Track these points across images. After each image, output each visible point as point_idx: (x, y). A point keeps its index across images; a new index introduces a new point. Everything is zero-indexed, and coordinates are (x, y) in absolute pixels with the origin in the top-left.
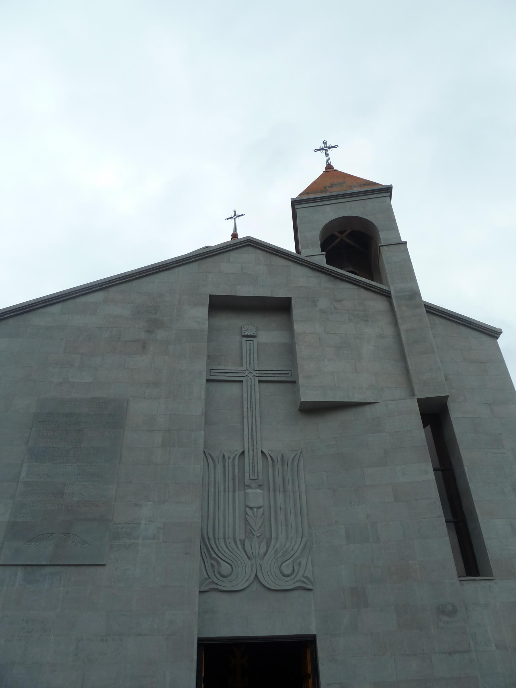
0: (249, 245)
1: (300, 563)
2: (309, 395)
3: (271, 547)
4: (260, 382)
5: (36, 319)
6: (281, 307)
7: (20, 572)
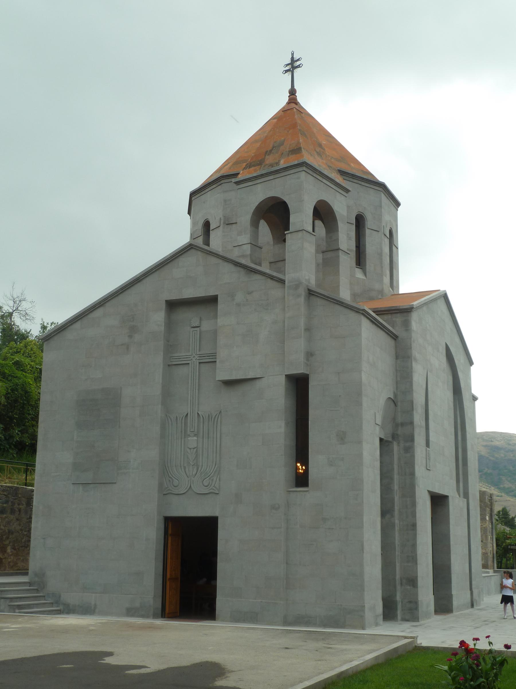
0: (192, 248)
1: (213, 480)
3: (199, 471)
4: (199, 363)
5: (69, 335)
7: (81, 487)
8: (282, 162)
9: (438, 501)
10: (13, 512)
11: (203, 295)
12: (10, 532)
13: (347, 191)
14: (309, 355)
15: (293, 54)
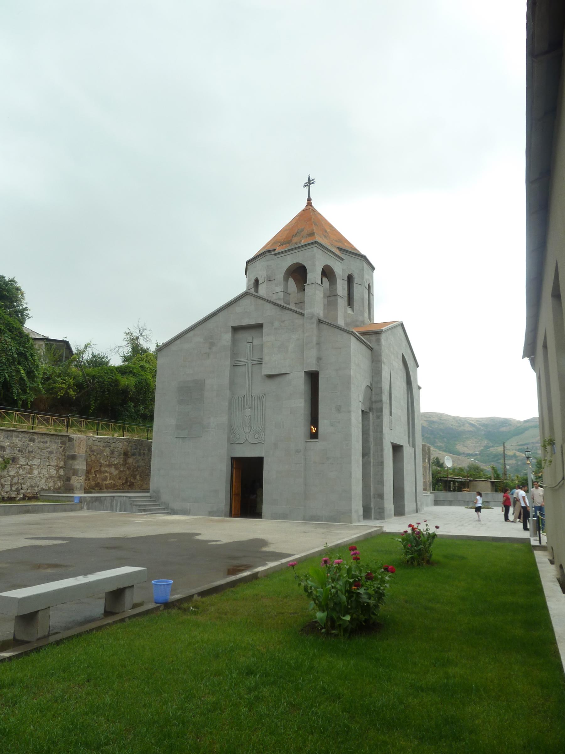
5: (173, 348)
8: (302, 241)
9: (397, 449)
10: (140, 455)
12: (139, 467)
13: (343, 259)
14: (319, 359)
15: (309, 177)
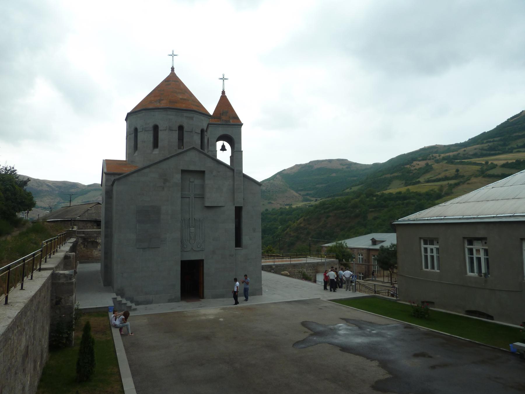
2: (207, 204)
6: (202, 173)
8: (231, 121)
11: (198, 169)
